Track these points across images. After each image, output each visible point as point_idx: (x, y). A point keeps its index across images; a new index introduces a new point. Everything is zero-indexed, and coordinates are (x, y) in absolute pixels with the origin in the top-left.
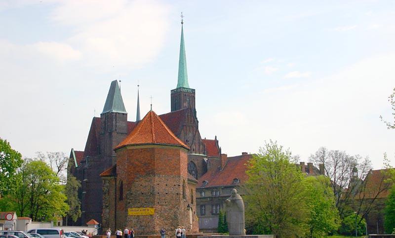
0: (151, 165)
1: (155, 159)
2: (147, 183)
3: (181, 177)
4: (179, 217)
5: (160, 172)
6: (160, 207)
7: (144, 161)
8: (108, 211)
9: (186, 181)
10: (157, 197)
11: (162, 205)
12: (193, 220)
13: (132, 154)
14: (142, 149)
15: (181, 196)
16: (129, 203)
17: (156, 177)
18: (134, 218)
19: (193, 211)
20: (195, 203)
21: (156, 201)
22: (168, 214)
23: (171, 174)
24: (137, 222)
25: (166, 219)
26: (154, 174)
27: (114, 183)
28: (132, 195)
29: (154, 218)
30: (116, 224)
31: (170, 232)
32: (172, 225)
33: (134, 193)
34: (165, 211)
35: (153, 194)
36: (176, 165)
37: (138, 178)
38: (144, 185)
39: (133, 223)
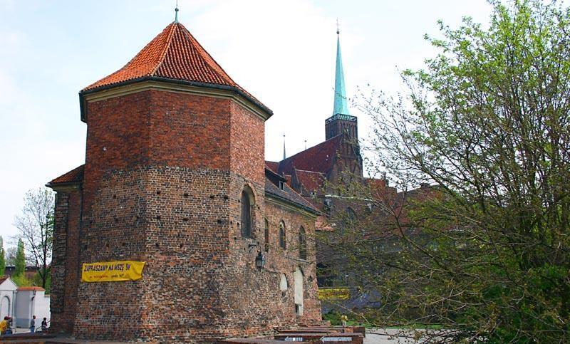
0: (139, 139)
4: (225, 290)
5: (165, 157)
7: (124, 129)
9: (259, 193)
10: (153, 228)
11: (172, 253)
12: (306, 295)
15: (234, 229)
17: (154, 174)
18: (94, 291)
20: (312, 258)
21: (151, 240)
22: (189, 279)
24: (101, 301)
25: (181, 293)
26: (146, 163)
27: (79, 202)
28: (95, 227)
29: (141, 291)
32: (200, 311)
33: (98, 221)
34: (179, 269)
35: (143, 221)
36: (218, 140)
37: (108, 177)
39: (91, 304)
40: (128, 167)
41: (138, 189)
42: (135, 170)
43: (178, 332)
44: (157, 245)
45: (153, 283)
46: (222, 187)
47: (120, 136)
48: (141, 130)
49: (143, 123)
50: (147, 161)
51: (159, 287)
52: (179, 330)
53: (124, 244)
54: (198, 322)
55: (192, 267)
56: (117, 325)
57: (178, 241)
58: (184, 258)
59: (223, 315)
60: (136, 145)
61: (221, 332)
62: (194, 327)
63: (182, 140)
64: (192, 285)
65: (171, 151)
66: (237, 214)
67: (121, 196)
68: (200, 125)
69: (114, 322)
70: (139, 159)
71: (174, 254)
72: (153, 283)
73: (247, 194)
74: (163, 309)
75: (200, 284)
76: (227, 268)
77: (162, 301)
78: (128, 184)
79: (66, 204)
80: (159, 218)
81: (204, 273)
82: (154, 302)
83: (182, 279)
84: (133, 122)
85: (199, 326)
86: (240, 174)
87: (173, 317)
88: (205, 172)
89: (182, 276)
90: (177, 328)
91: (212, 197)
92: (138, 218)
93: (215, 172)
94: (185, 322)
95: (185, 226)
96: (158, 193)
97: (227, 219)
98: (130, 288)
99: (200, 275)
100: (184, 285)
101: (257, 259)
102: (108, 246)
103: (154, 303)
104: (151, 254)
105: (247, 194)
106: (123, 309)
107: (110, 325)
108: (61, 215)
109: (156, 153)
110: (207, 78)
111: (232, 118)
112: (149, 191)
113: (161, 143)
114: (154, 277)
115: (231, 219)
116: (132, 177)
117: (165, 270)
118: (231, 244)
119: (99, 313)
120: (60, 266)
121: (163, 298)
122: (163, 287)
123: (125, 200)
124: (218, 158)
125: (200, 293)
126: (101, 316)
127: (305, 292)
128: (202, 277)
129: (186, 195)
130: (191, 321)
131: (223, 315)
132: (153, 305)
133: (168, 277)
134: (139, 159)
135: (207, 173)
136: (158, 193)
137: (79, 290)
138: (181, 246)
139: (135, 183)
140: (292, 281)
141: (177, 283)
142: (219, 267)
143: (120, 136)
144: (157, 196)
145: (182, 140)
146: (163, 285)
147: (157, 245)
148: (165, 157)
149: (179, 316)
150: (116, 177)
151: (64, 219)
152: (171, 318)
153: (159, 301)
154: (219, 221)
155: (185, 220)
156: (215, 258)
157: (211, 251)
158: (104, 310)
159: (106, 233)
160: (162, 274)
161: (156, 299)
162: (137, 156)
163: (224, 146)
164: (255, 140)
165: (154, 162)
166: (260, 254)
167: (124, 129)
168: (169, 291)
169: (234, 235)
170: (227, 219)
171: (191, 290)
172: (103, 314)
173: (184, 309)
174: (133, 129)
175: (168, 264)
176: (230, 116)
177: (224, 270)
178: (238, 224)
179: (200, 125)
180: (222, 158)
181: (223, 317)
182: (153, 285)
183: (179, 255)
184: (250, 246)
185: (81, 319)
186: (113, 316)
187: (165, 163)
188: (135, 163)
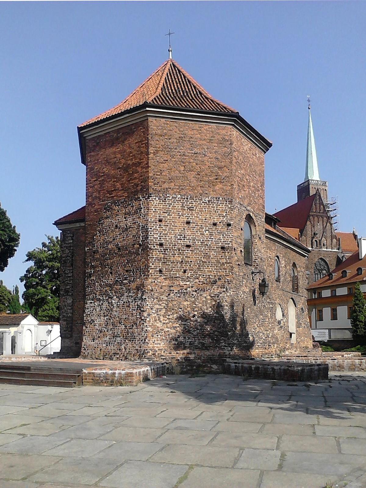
0: (139, 169)
1: (151, 150)
2: (130, 219)
6: (166, 283)
14: (118, 131)
15: (238, 256)
17: (155, 201)
22: (194, 302)
29: (145, 314)
35: (145, 248)
36: (220, 168)
41: (139, 218)
44: (160, 271)
45: (157, 306)
46: (224, 214)
48: (141, 159)
49: (142, 153)
51: (164, 311)
53: (127, 271)
54: (203, 344)
55: (196, 291)
56: (123, 347)
57: (182, 267)
58: (188, 283)
62: (199, 348)
63: (182, 168)
64: (197, 309)
65: (171, 180)
66: (240, 241)
67: (122, 225)
68: (200, 154)
69: (120, 344)
70: (139, 188)
71: (177, 279)
72: (157, 306)
74: (168, 331)
75: (205, 307)
76: (232, 293)
77: (167, 323)
78: (129, 214)
80: (161, 245)
81: (209, 297)
82: (159, 325)
83: (186, 303)
84: (131, 152)
86: (242, 203)
87: (178, 339)
88: (207, 199)
91: (215, 224)
92: (140, 245)
95: (188, 252)
97: (230, 245)
99: (204, 299)
100: (189, 309)
102: (111, 273)
103: (158, 325)
104: (155, 279)
110: (208, 106)
111: (233, 146)
112: (152, 217)
114: (158, 301)
115: (235, 246)
116: (133, 206)
117: (169, 295)
118: (236, 270)
121: (168, 321)
122: (167, 310)
124: (221, 186)
128: (206, 302)
129: (188, 223)
130: (196, 343)
132: (158, 327)
133: (172, 301)
134: (139, 188)
135: (209, 201)
136: (160, 221)
137: (84, 315)
138: (185, 272)
139: (136, 212)
141: (182, 306)
142: (224, 291)
144: (158, 223)
145: (182, 168)
146: (167, 309)
147: (160, 271)
148: (166, 186)
149: (185, 338)
152: (176, 340)
153: (164, 323)
155: (188, 246)
156: (219, 283)
157: (215, 276)
160: (166, 298)
161: (161, 321)
162: (137, 185)
163: (225, 174)
164: (255, 171)
165: (155, 190)
167: (123, 161)
168: (173, 314)
169: (238, 261)
170: (230, 245)
171: (196, 313)
174: (132, 159)
175: (172, 289)
176: (231, 144)
177: (228, 294)
178: (241, 251)
179: (200, 154)
180: (224, 185)
182: (157, 309)
183: (183, 280)
185: (87, 341)
188: (136, 192)
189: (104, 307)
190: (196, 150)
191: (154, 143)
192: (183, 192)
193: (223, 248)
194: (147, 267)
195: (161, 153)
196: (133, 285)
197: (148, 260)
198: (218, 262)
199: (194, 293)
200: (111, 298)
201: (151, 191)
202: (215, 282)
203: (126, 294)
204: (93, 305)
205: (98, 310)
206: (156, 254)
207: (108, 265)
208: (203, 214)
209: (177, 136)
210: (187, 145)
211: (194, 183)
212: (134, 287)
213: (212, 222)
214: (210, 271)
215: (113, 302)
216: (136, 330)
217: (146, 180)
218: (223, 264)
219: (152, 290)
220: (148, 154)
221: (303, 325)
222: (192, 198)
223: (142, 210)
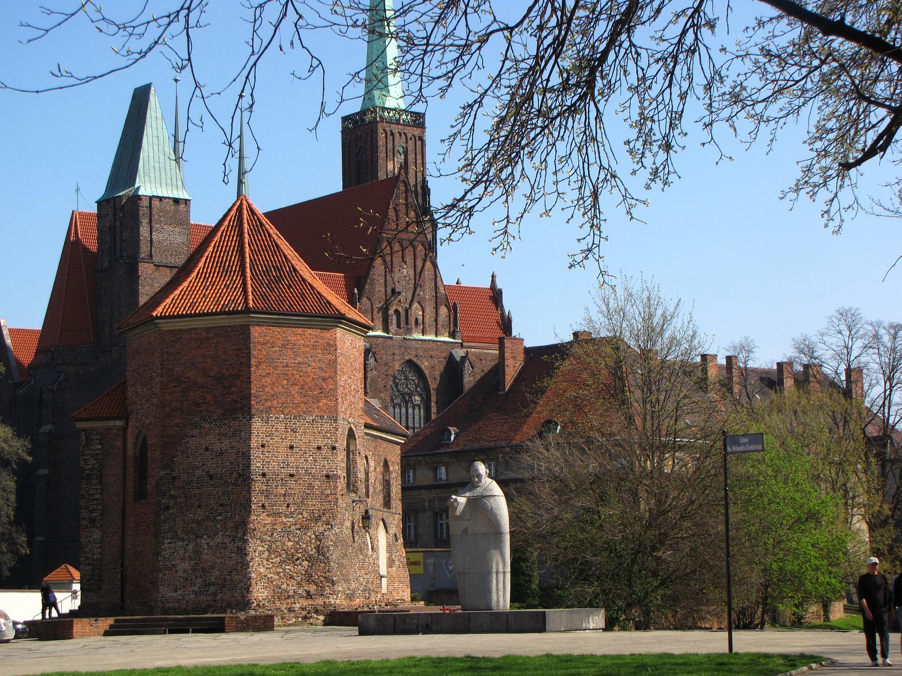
0: (238, 383)
1: (253, 362)
3: (340, 422)
4: (334, 555)
5: (269, 404)
6: (269, 520)
8: (97, 535)
13: (178, 346)
15: (341, 484)
16: (167, 508)
17: (257, 424)
19: (392, 531)
20: (397, 505)
21: (257, 499)
23: (310, 413)
24: (194, 570)
25: (292, 559)
27: (119, 443)
30: (123, 580)
31: (305, 603)
34: (287, 532)
36: (324, 379)
38: (216, 447)
39: (180, 574)
40: (224, 415)
42: (234, 419)
43: (288, 603)
44: (263, 506)
45: (260, 548)
47: (210, 376)
49: (242, 363)
50: (250, 408)
52: (289, 601)
53: (222, 505)
54: (308, 592)
56: (219, 597)
59: (333, 583)
60: (234, 389)
61: (333, 602)
63: (285, 382)
69: (215, 594)
72: (260, 548)
73: (351, 435)
78: (225, 435)
79: (99, 447)
80: (264, 475)
82: (262, 570)
83: (290, 544)
85: (309, 595)
89: (289, 540)
90: (286, 599)
91: (319, 448)
92: (239, 474)
93: (322, 417)
94: (294, 592)
95: (291, 482)
96: (263, 446)
98: (233, 555)
101: (363, 518)
102: (199, 506)
104: (258, 516)
105: (351, 435)
106: (225, 579)
107: (209, 598)
108: (92, 461)
109: (258, 400)
111: (338, 351)
112: (254, 442)
113: (264, 386)
116: (230, 427)
119: (192, 584)
120: (94, 529)
122: (270, 553)
123: (221, 454)
125: (310, 559)
126: (196, 588)
127: (389, 558)
129: (291, 447)
130: (300, 591)
131: (333, 583)
136: (263, 446)
138: (288, 506)
139: (234, 435)
140: (376, 542)
141: (285, 548)
143: (210, 376)
148: (269, 404)
150: (208, 426)
151: (96, 466)
154: (327, 476)
155: (292, 475)
156: (324, 519)
158: (199, 580)
159: (197, 492)
166: (367, 512)
172: (198, 585)
173: (292, 577)
174: (228, 369)
176: (336, 350)
181: (333, 585)
184: (353, 501)
186: (212, 588)
187: (268, 410)
189: (190, 547)
190: (299, 359)
191: (257, 352)
192: (286, 411)
193: (327, 476)
194: (249, 502)
195: (263, 366)
196: (230, 524)
197: (250, 494)
198: (322, 493)
199: (298, 532)
200: (201, 537)
201: (253, 411)
202: (320, 516)
203: (220, 534)
204: (172, 545)
205: (181, 553)
206: (258, 486)
207: (195, 496)
208: (306, 438)
209: (279, 343)
210: (290, 353)
211: (298, 399)
212: (232, 525)
213: (315, 445)
214: (314, 504)
215: (203, 541)
216: (236, 577)
217: (247, 397)
218: (328, 496)
219: (255, 530)
220: (250, 367)
221: (397, 563)
222: (295, 418)
223: (243, 433)
